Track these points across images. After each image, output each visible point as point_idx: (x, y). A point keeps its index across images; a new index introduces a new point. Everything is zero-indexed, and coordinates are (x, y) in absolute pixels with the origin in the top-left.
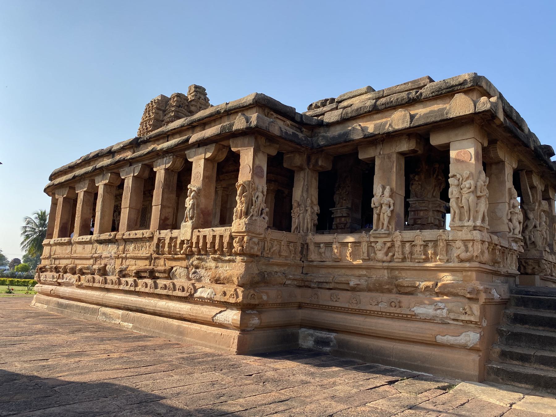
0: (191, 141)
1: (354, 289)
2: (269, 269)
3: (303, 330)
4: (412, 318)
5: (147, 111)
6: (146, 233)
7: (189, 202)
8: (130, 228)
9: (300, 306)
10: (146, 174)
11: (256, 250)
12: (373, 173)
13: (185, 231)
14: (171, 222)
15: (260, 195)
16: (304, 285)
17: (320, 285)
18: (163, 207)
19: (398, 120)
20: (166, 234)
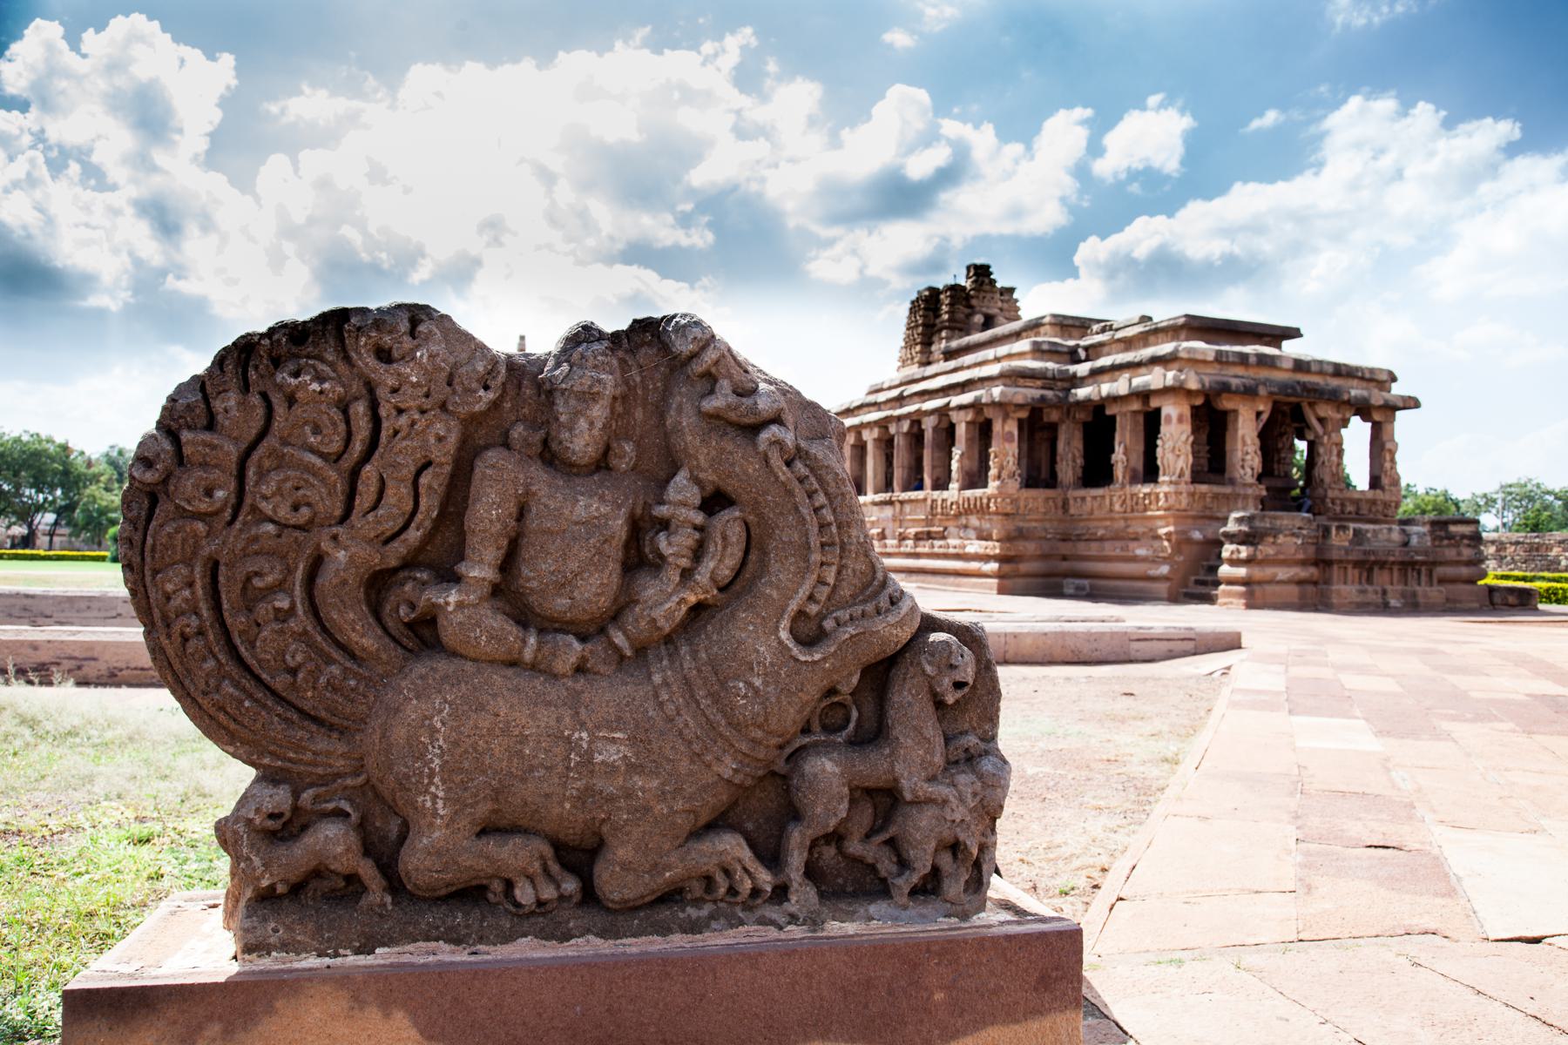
0: (953, 404)
1: (1101, 539)
2: (1026, 525)
3: (1070, 580)
4: (1135, 559)
5: (913, 310)
6: (919, 495)
7: (955, 465)
8: (905, 489)
9: (1065, 558)
10: (915, 429)
11: (1009, 509)
12: (1114, 430)
13: (953, 493)
14: (941, 484)
15: (1011, 459)
16: (1065, 539)
17: (1079, 538)
18: (934, 467)
19: (1120, 386)
20: (936, 494)
